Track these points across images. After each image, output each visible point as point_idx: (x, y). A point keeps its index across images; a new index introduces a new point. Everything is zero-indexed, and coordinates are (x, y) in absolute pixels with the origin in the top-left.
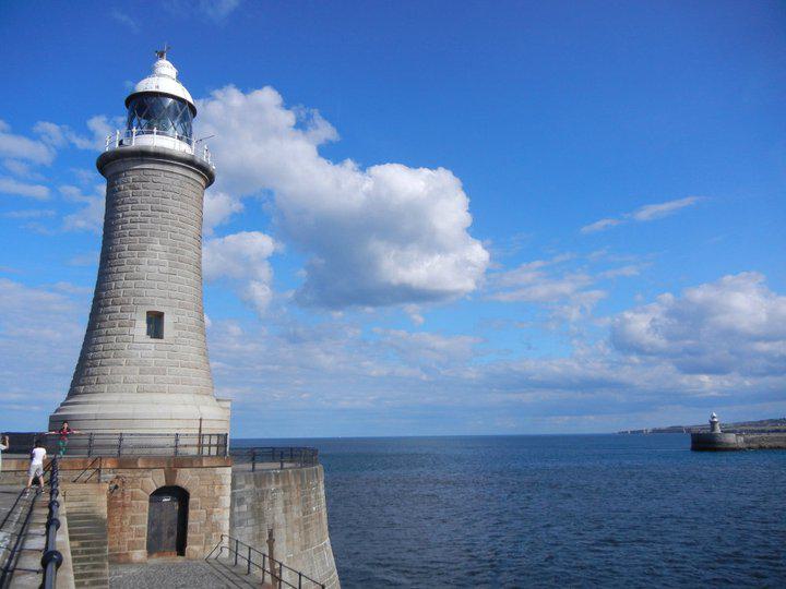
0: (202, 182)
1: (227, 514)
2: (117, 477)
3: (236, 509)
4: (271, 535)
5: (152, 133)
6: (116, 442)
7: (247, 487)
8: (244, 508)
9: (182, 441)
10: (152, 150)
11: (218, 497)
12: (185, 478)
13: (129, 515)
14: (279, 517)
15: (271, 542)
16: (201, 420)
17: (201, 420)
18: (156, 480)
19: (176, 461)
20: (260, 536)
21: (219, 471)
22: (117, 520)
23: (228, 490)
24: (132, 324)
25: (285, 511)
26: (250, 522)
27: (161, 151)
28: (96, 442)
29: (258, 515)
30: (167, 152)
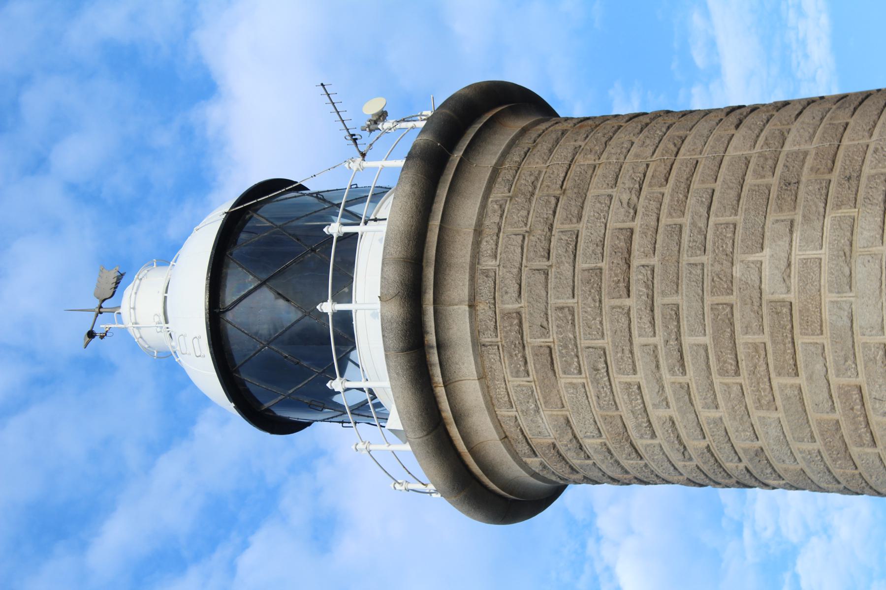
0: (515, 126)
5: (345, 321)
10: (396, 310)
27: (394, 274)
30: (398, 251)
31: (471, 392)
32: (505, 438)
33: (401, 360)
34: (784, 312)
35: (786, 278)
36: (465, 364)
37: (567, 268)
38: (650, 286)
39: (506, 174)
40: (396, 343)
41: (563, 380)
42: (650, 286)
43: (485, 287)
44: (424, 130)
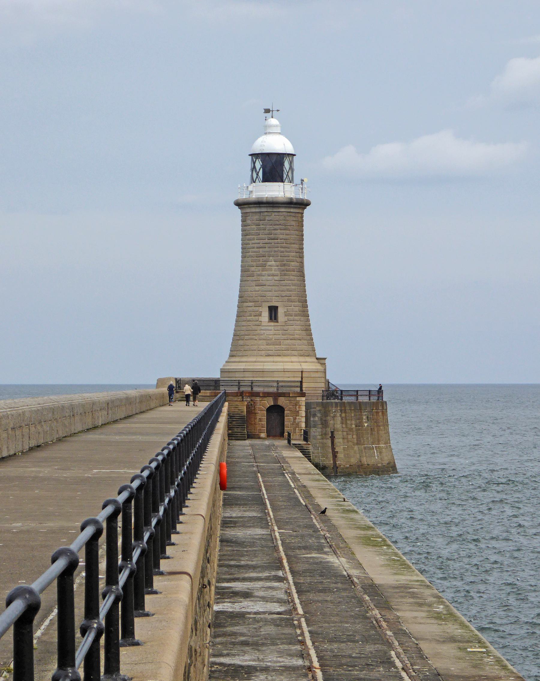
1: (304, 420)
2: (252, 400)
3: (312, 419)
4: (332, 433)
6: (250, 384)
7: (318, 408)
8: (317, 419)
9: (280, 384)
10: (265, 200)
11: (298, 412)
12: (282, 401)
13: (258, 417)
14: (338, 426)
15: (333, 437)
16: (302, 372)
17: (302, 372)
18: (269, 402)
19: (276, 396)
20: (325, 434)
21: (298, 399)
22: (253, 419)
23: (304, 408)
24: (260, 315)
25: (342, 423)
26: (320, 426)
27: (271, 200)
28: (241, 384)
29: (325, 424)
30: (275, 200)
31: (253, 210)
32: (247, 213)
33: (256, 200)
34: (264, 266)
35: (269, 266)
36: (257, 210)
37: (272, 229)
38: (269, 243)
39: (289, 214)
40: (260, 200)
41: (255, 226)
42: (269, 243)
43: (269, 214)
44: (296, 199)
